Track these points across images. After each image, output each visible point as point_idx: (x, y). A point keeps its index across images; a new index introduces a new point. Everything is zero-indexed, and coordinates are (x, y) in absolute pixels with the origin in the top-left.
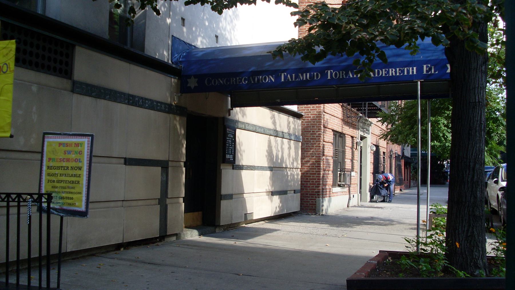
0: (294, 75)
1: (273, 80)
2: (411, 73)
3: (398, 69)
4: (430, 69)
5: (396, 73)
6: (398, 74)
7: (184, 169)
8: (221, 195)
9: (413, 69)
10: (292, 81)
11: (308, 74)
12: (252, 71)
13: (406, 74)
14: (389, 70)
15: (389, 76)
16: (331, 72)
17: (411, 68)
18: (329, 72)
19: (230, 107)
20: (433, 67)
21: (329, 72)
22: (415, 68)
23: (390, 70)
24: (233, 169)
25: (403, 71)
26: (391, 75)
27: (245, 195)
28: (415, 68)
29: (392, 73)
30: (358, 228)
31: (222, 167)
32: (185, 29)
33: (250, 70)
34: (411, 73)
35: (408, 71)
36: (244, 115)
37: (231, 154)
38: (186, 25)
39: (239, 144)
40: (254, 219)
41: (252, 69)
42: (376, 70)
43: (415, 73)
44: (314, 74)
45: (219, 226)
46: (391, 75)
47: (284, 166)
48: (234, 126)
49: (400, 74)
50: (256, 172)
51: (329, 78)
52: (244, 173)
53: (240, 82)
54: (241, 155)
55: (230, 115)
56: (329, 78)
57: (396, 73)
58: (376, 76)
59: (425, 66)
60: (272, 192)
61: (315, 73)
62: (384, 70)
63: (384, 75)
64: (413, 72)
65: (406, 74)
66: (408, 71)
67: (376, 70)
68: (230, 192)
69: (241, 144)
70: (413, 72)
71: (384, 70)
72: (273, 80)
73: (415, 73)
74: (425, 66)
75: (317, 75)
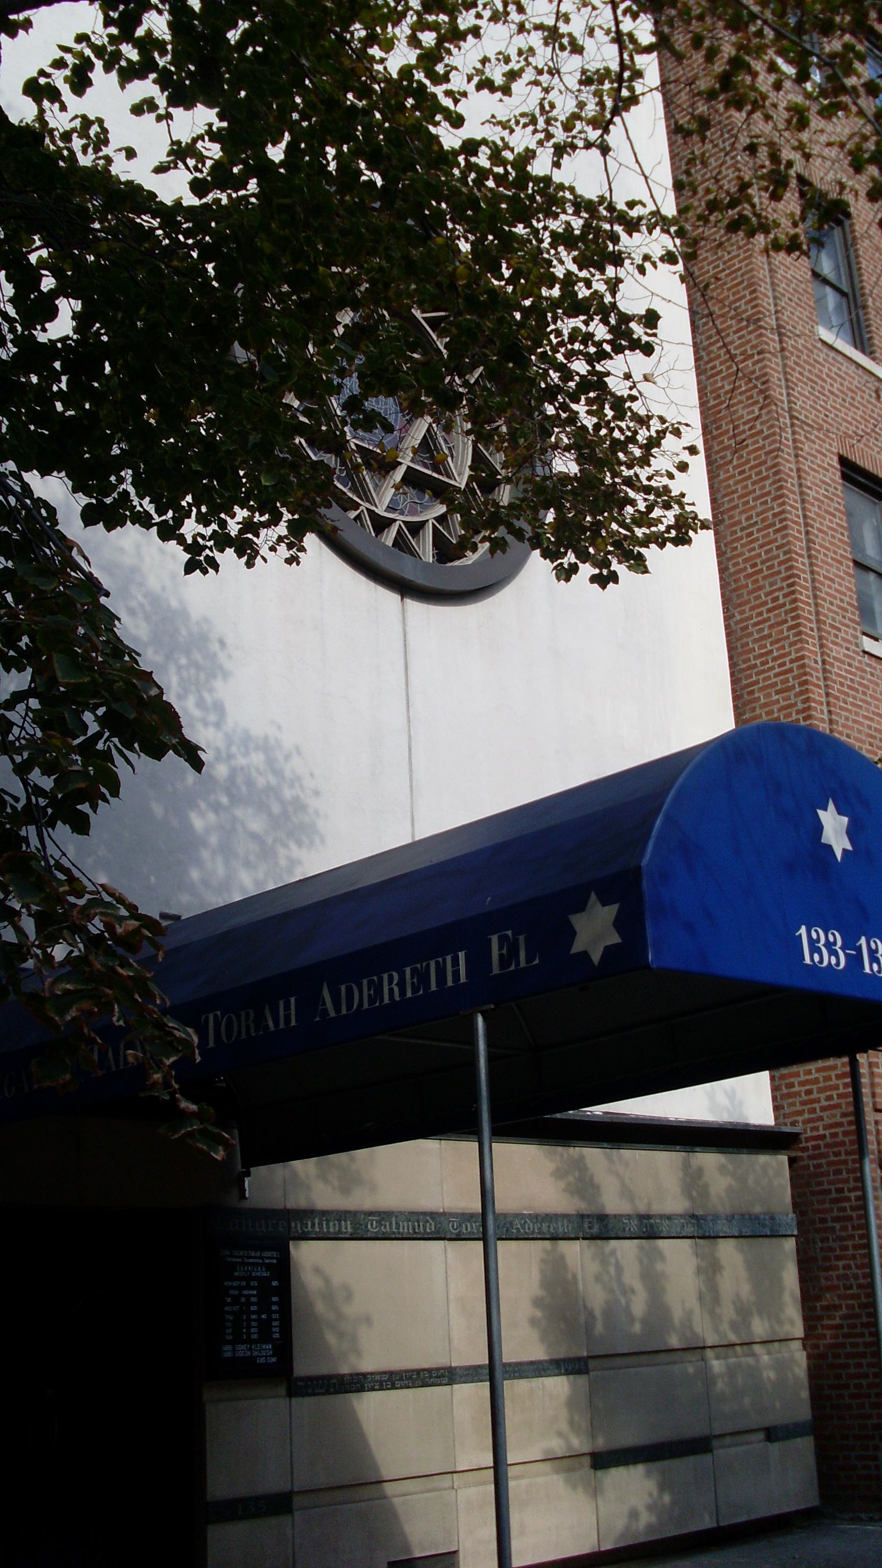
2: (450, 983)
3: (408, 971)
5: (403, 992)
6: (409, 994)
9: (455, 962)
13: (433, 987)
16: (216, 1016)
17: (449, 958)
18: (211, 1016)
19: (239, 1168)
20: (522, 938)
21: (211, 1016)
22: (462, 955)
23: (385, 976)
24: (290, 1394)
25: (424, 978)
28: (462, 955)
29: (391, 991)
34: (450, 983)
37: (265, 1337)
39: (329, 1296)
42: (343, 988)
43: (463, 979)
47: (674, 1341)
49: (415, 990)
52: (370, 1407)
54: (341, 1335)
57: (403, 992)
58: (344, 1012)
59: (495, 939)
62: (365, 982)
64: (456, 974)
65: (433, 987)
67: (343, 988)
68: (273, 1482)
71: (365, 982)
73: (463, 979)
74: (495, 939)
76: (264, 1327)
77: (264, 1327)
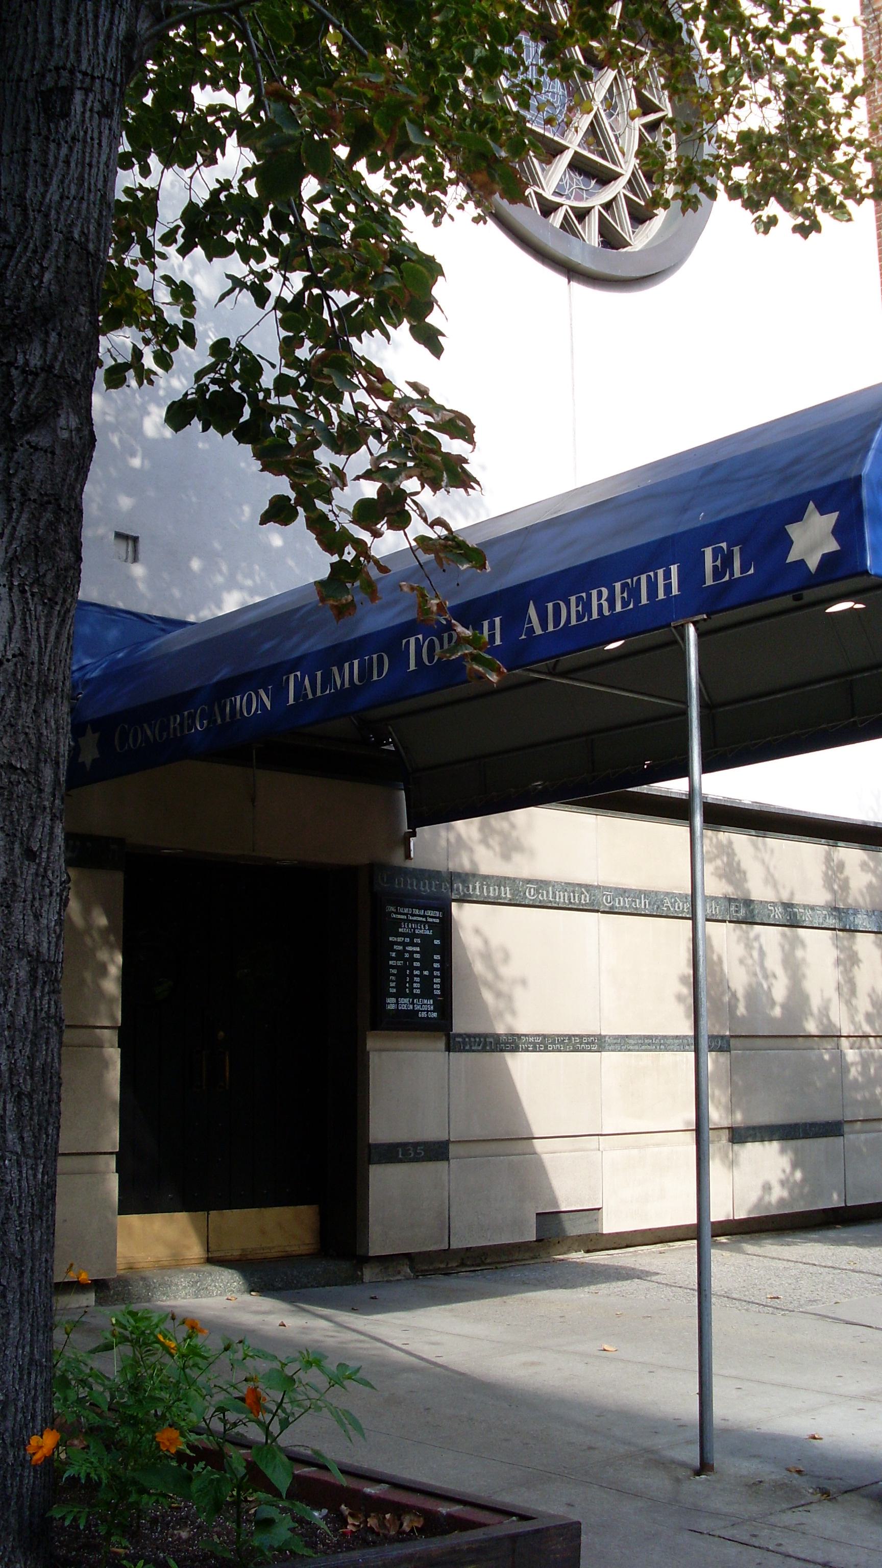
0: (319, 673)
1: (268, 704)
2: (661, 595)
3: (618, 586)
4: (728, 561)
5: (612, 606)
6: (619, 608)
7: (114, 1054)
8: (369, 1145)
9: (667, 575)
10: (316, 699)
11: (356, 662)
12: (217, 683)
13: (644, 600)
14: (589, 596)
15: (592, 623)
16: (417, 640)
17: (660, 572)
18: (412, 640)
19: (405, 828)
20: (736, 550)
21: (412, 640)
22: (674, 569)
23: (594, 593)
24: (448, 1049)
25: (634, 593)
26: (595, 616)
27: (539, 1146)
28: (674, 569)
29: (600, 606)
30: (604, 1288)
31: (370, 1044)
32: (138, 570)
33: (215, 680)
34: (661, 595)
35: (652, 587)
36: (510, 847)
37: (427, 992)
38: (141, 556)
39: (487, 956)
40: (605, 1232)
41: (224, 673)
42: (550, 606)
43: (675, 591)
44: (371, 659)
45: (367, 1260)
46: (595, 616)
47: (812, 1027)
48: (440, 894)
49: (625, 604)
50: (610, 1058)
51: (412, 667)
52: (522, 1067)
53: (190, 729)
54: (499, 994)
55: (408, 856)
56: (412, 667)
57: (612, 606)
58: (551, 628)
59: (708, 552)
60: (732, 1129)
61: (375, 656)
62: (573, 599)
63: (574, 622)
64: (668, 587)
65: (644, 600)
66: (652, 587)
67: (550, 606)
68: (432, 1133)
69: (498, 956)
70: (668, 587)
71: (573, 599)
72: (268, 704)
73: (675, 591)
74: (708, 552)
75: (381, 660)
76: (427, 983)
77: (427, 983)
